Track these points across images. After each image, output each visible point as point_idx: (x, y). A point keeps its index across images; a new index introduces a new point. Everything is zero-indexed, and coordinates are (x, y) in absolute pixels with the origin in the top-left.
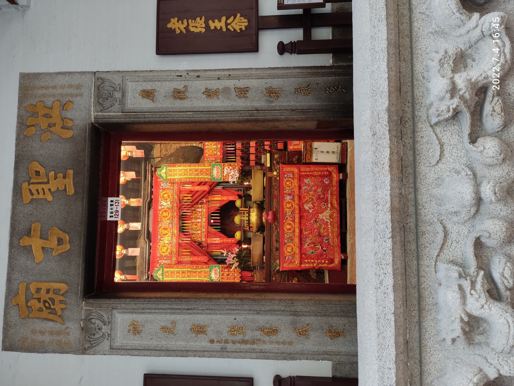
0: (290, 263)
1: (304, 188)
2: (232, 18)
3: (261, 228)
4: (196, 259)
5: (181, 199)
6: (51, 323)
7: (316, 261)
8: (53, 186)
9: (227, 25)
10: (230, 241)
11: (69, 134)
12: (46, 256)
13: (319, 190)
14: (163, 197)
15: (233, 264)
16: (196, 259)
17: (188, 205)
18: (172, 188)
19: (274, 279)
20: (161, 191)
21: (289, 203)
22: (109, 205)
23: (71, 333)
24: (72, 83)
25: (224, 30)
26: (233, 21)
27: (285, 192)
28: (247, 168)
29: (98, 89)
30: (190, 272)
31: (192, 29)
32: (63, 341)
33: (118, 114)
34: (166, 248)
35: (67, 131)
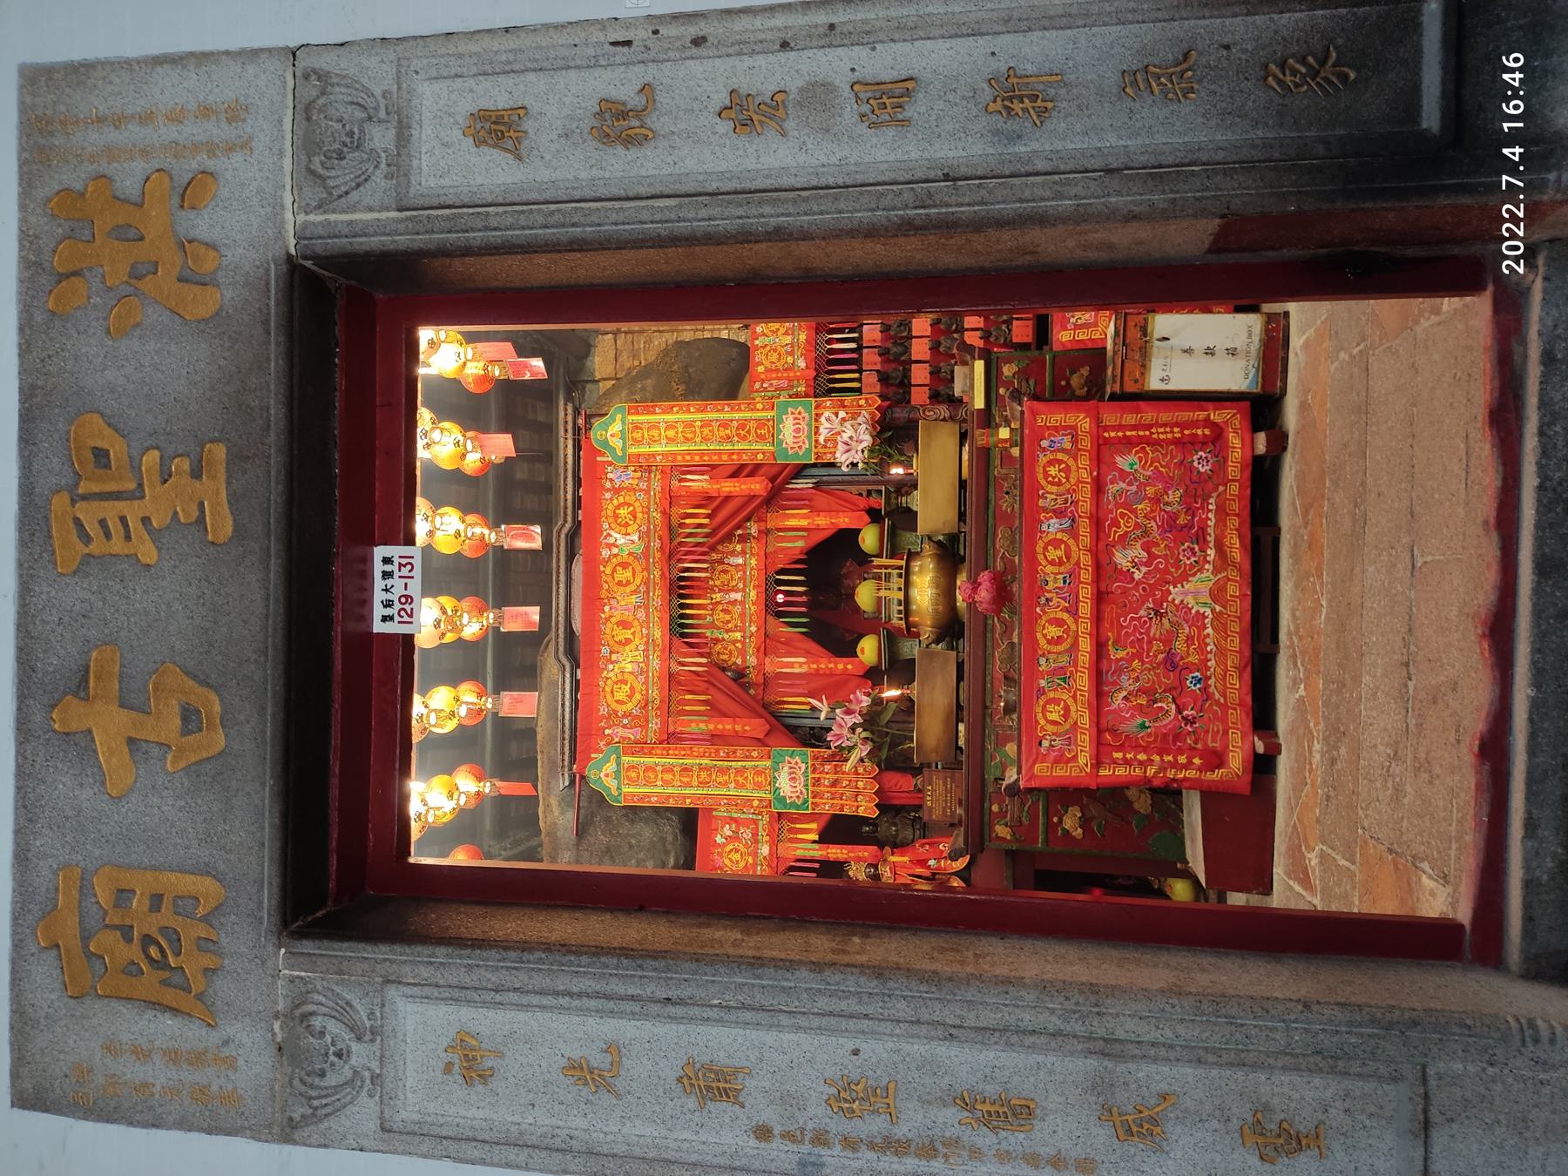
0: (1057, 761)
1: (1112, 489)
3: (950, 628)
4: (727, 726)
5: (674, 522)
6: (169, 1022)
7: (1156, 758)
8: (158, 505)
10: (840, 666)
11: (206, 303)
12: (141, 772)
13: (1174, 496)
14: (616, 516)
15: (850, 749)
16: (727, 726)
17: (698, 544)
18: (643, 485)
19: (995, 808)
20: (608, 495)
21: (1056, 543)
22: (378, 575)
23: (241, 1062)
24: (211, 99)
27: (1041, 503)
28: (900, 414)
29: (308, 119)
30: (707, 768)
32: (215, 1088)
33: (384, 215)
34: (627, 688)
35: (197, 289)
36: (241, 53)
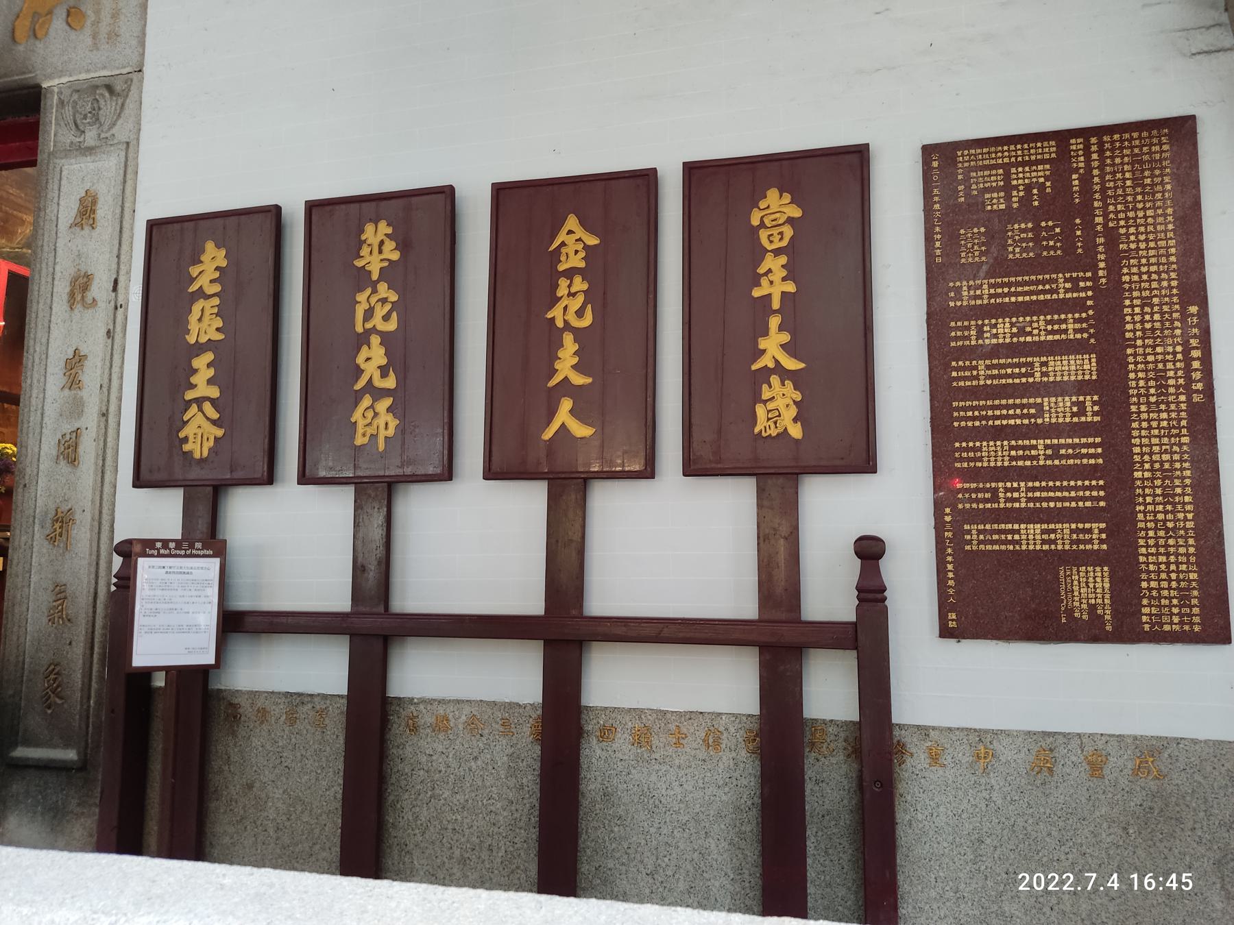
2: (215, 416)
9: (199, 401)
24: (122, 17)
25: (190, 395)
26: (208, 418)
31: (196, 308)
36: (144, 34)
